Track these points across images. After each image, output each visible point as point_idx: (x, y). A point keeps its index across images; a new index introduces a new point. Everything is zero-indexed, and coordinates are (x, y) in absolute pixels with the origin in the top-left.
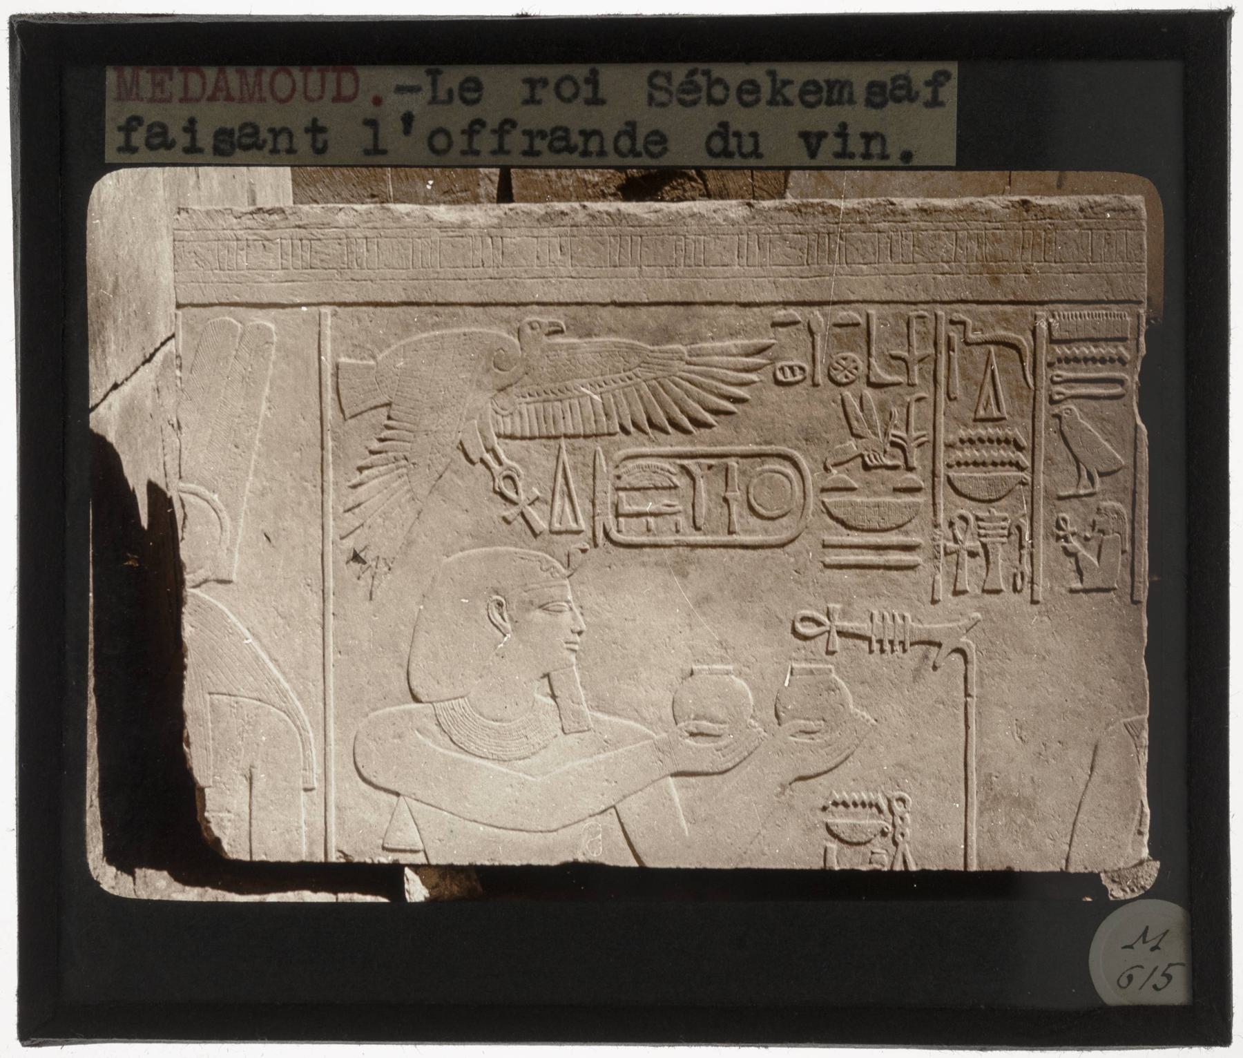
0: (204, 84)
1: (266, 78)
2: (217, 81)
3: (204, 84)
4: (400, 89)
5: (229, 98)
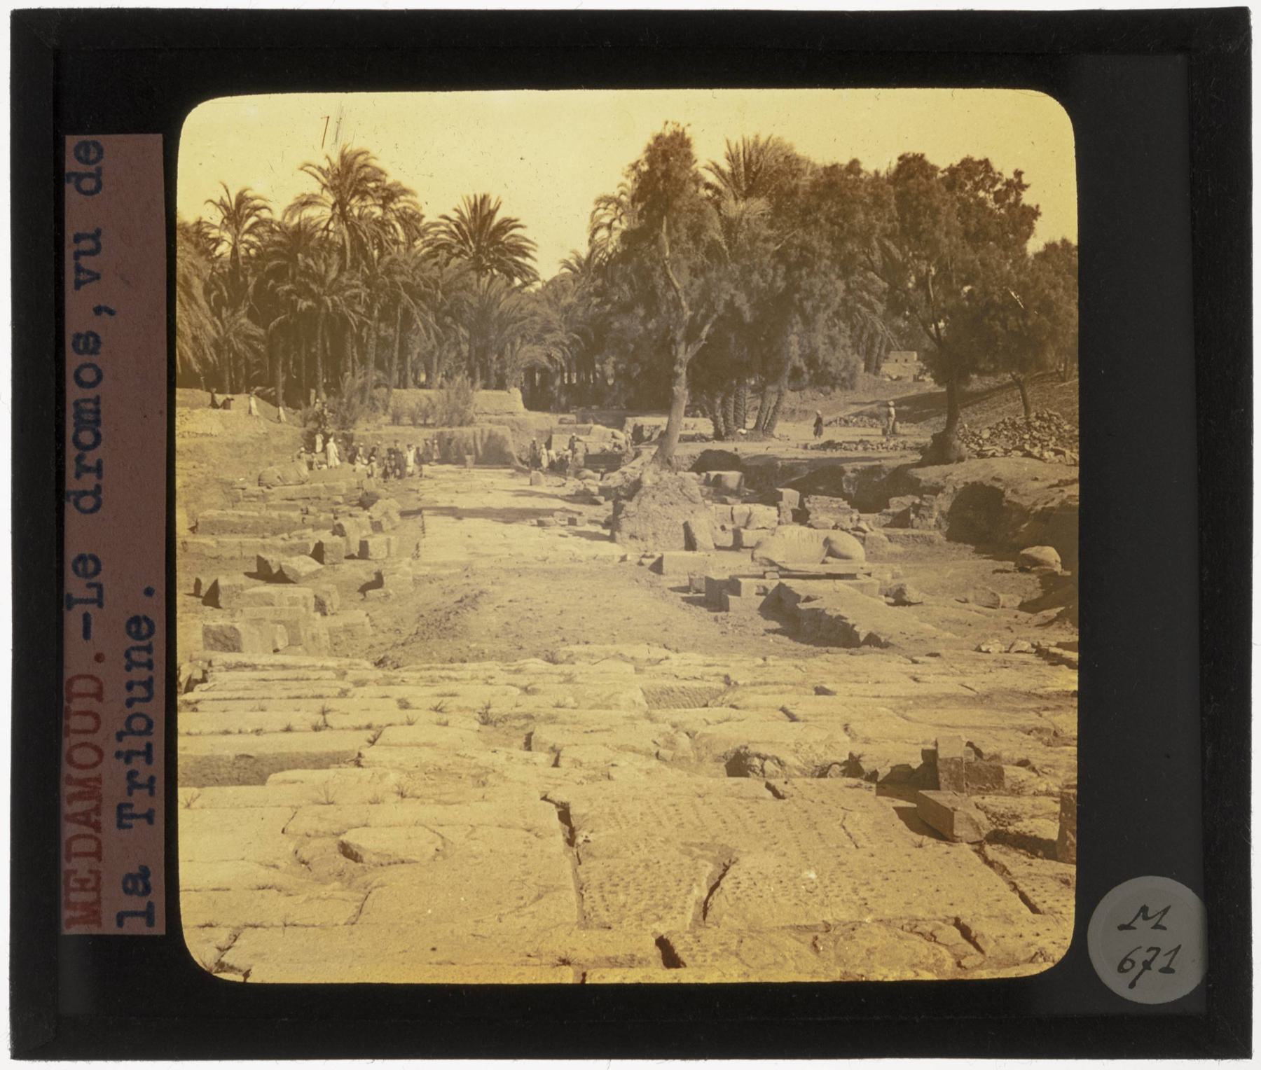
0: (85, 836)
1: (76, 773)
2: (79, 822)
3: (85, 836)
4: (86, 633)
5: (97, 810)
